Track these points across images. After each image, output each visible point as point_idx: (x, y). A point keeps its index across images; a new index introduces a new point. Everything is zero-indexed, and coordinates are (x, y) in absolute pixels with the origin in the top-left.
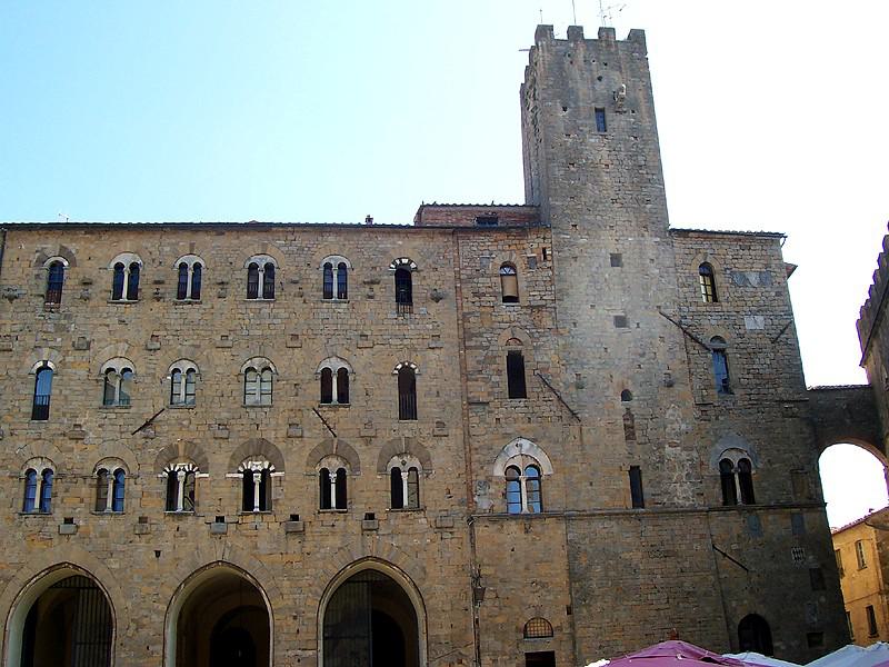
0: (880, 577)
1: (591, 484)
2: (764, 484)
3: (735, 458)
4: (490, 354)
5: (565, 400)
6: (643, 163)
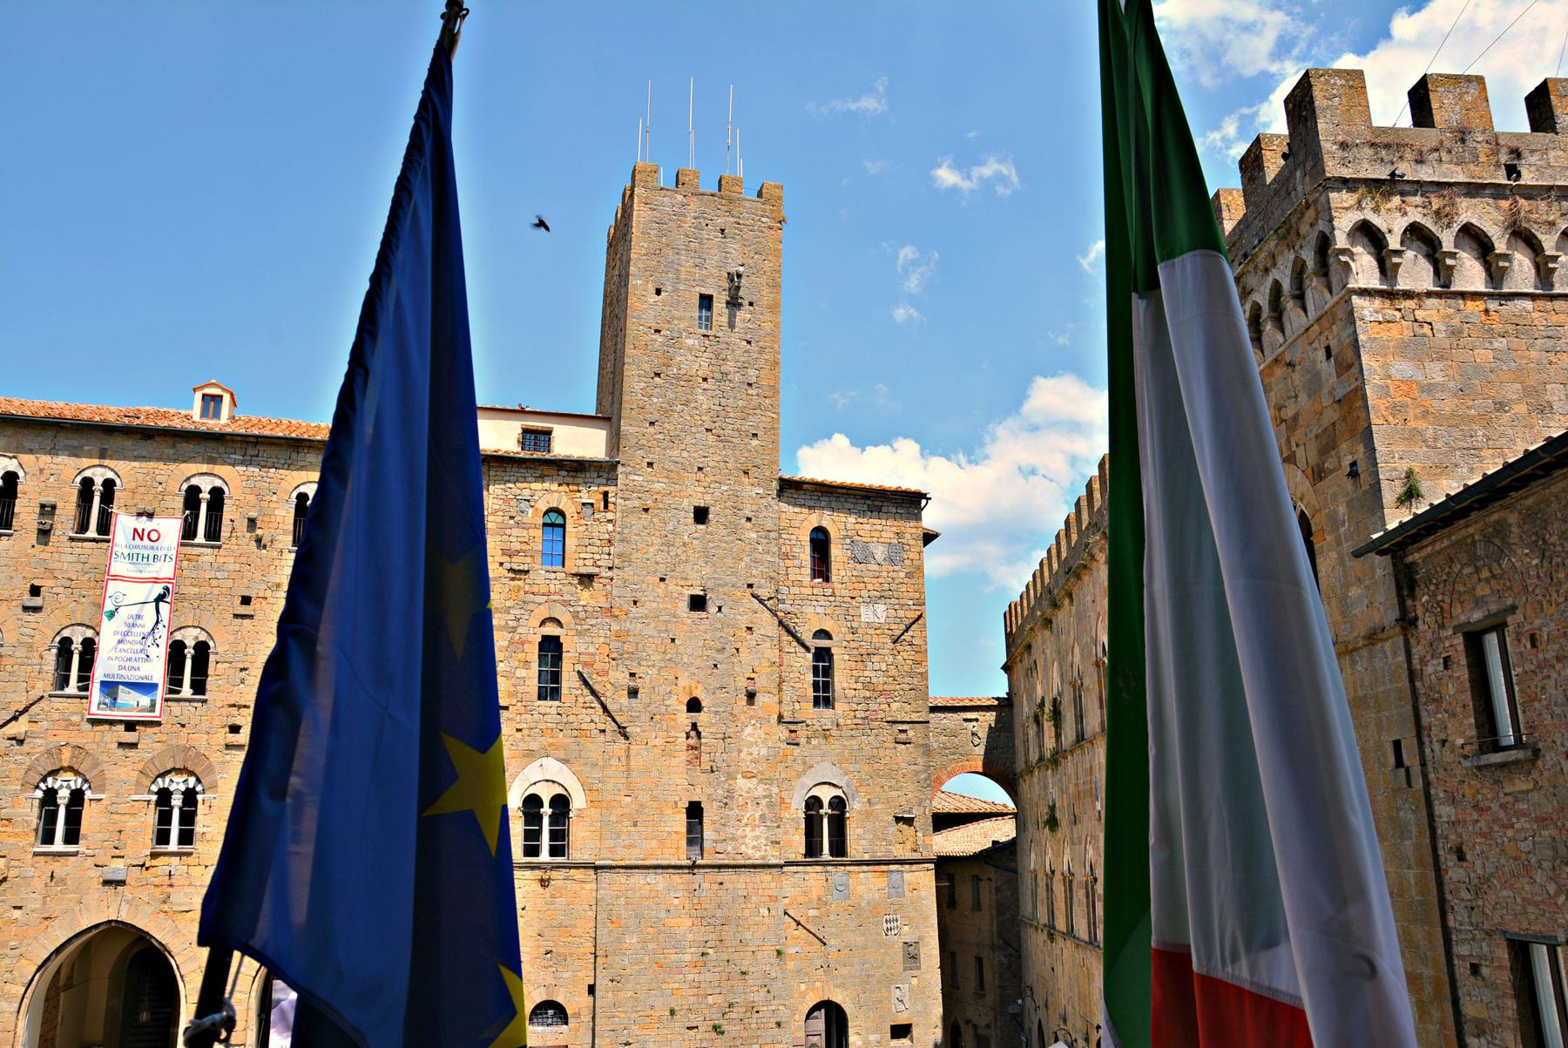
0: (995, 928)
1: (635, 825)
2: (860, 831)
3: (826, 794)
4: (517, 637)
5: (610, 707)
6: (754, 380)
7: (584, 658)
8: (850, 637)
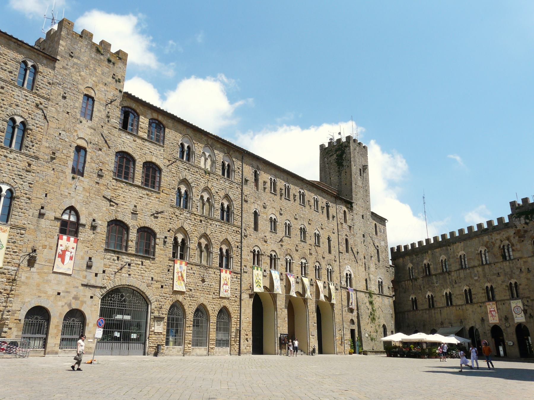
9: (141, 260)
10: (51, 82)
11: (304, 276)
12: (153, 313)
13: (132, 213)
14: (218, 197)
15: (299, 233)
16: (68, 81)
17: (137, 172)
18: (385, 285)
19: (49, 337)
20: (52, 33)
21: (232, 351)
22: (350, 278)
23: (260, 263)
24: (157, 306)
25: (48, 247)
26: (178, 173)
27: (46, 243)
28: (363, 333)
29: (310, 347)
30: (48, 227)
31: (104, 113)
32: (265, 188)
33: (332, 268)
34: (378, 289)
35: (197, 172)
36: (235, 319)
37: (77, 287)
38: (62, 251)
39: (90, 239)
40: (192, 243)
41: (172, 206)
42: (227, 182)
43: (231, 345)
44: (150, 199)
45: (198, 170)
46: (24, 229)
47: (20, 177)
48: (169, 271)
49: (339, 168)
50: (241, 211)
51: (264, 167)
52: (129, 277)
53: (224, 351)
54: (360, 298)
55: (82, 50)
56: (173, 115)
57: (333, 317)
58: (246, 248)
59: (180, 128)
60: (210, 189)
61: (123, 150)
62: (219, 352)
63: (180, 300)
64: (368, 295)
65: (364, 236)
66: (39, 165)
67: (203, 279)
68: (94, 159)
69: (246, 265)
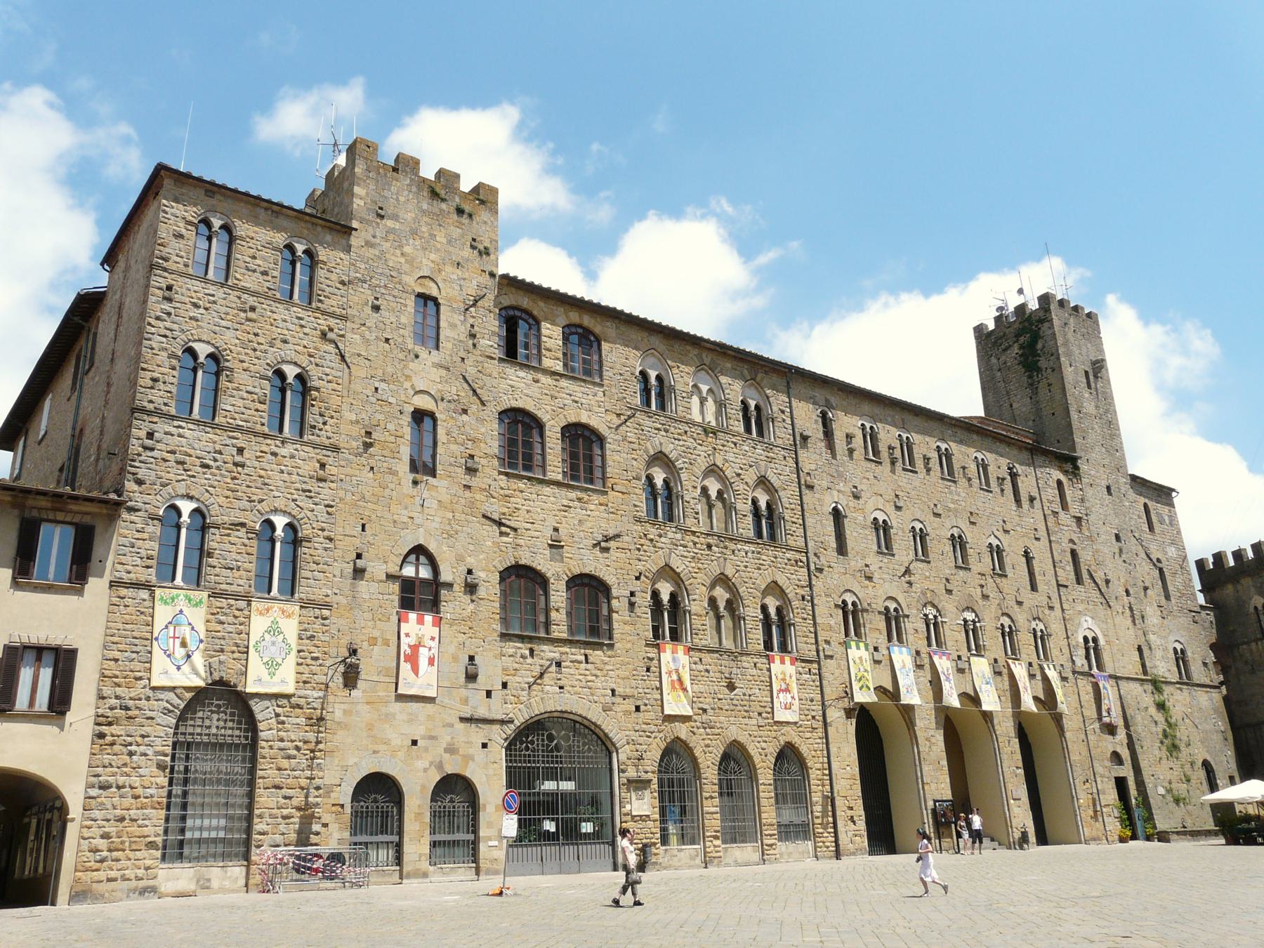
3: (1179, 647)
7: (1088, 563)
8: (1167, 563)
9: (583, 651)
10: (345, 279)
11: (974, 652)
12: (623, 771)
13: (551, 546)
14: (742, 486)
15: (949, 548)
16: (380, 271)
17: (550, 451)
18: (1194, 659)
19: (406, 839)
20: (336, 174)
21: (819, 849)
22: (1096, 649)
23: (863, 631)
24: (630, 754)
25: (380, 640)
26: (642, 442)
27: (376, 633)
28: (1150, 786)
29: (1015, 829)
30: (374, 597)
31: (462, 329)
32: (851, 451)
33: (1046, 628)
34: (1176, 669)
35: (686, 432)
36: (818, 772)
37: (452, 726)
38: (410, 646)
39: (465, 614)
40: (694, 600)
41: (639, 520)
42: (758, 447)
43: (814, 834)
44: (586, 510)
45: (687, 429)
46: (328, 606)
47: (307, 493)
48: (648, 670)
49: (1030, 377)
50: (800, 513)
51: (844, 400)
52: (561, 693)
53: (800, 850)
54: (1129, 697)
55: (402, 199)
56: (615, 308)
57: (1064, 750)
58: (824, 599)
59: (634, 337)
60: (721, 470)
61: (514, 406)
62: (790, 854)
63: (683, 737)
64: (1149, 687)
65: (1118, 538)
66: (342, 463)
67: (730, 682)
68: (454, 435)
69: (828, 639)
